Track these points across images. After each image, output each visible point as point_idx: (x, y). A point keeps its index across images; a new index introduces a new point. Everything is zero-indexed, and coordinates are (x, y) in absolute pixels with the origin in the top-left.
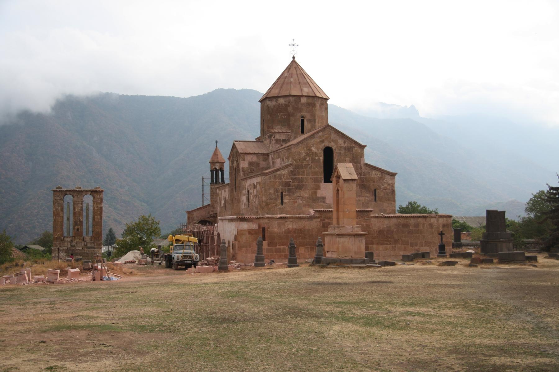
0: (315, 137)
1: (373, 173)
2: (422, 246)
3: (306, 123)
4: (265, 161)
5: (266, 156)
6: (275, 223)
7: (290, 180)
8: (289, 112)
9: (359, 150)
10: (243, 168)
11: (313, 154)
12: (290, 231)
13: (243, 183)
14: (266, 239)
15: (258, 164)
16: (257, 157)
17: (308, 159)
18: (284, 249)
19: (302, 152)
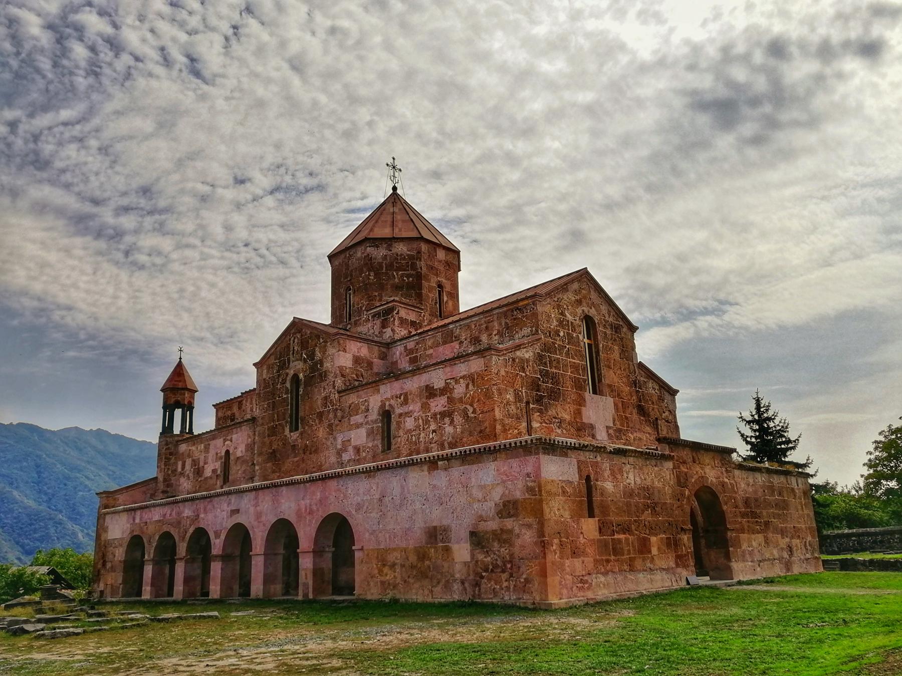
0: (568, 291)
1: (650, 384)
2: (792, 538)
3: (445, 299)
4: (382, 359)
5: (384, 350)
6: (606, 465)
7: (539, 376)
8: (419, 270)
9: (629, 334)
10: (341, 368)
11: (569, 327)
12: (632, 490)
13: (352, 398)
14: (597, 511)
15: (370, 364)
16: (368, 347)
17: (562, 334)
18: (627, 539)
19: (553, 316)
